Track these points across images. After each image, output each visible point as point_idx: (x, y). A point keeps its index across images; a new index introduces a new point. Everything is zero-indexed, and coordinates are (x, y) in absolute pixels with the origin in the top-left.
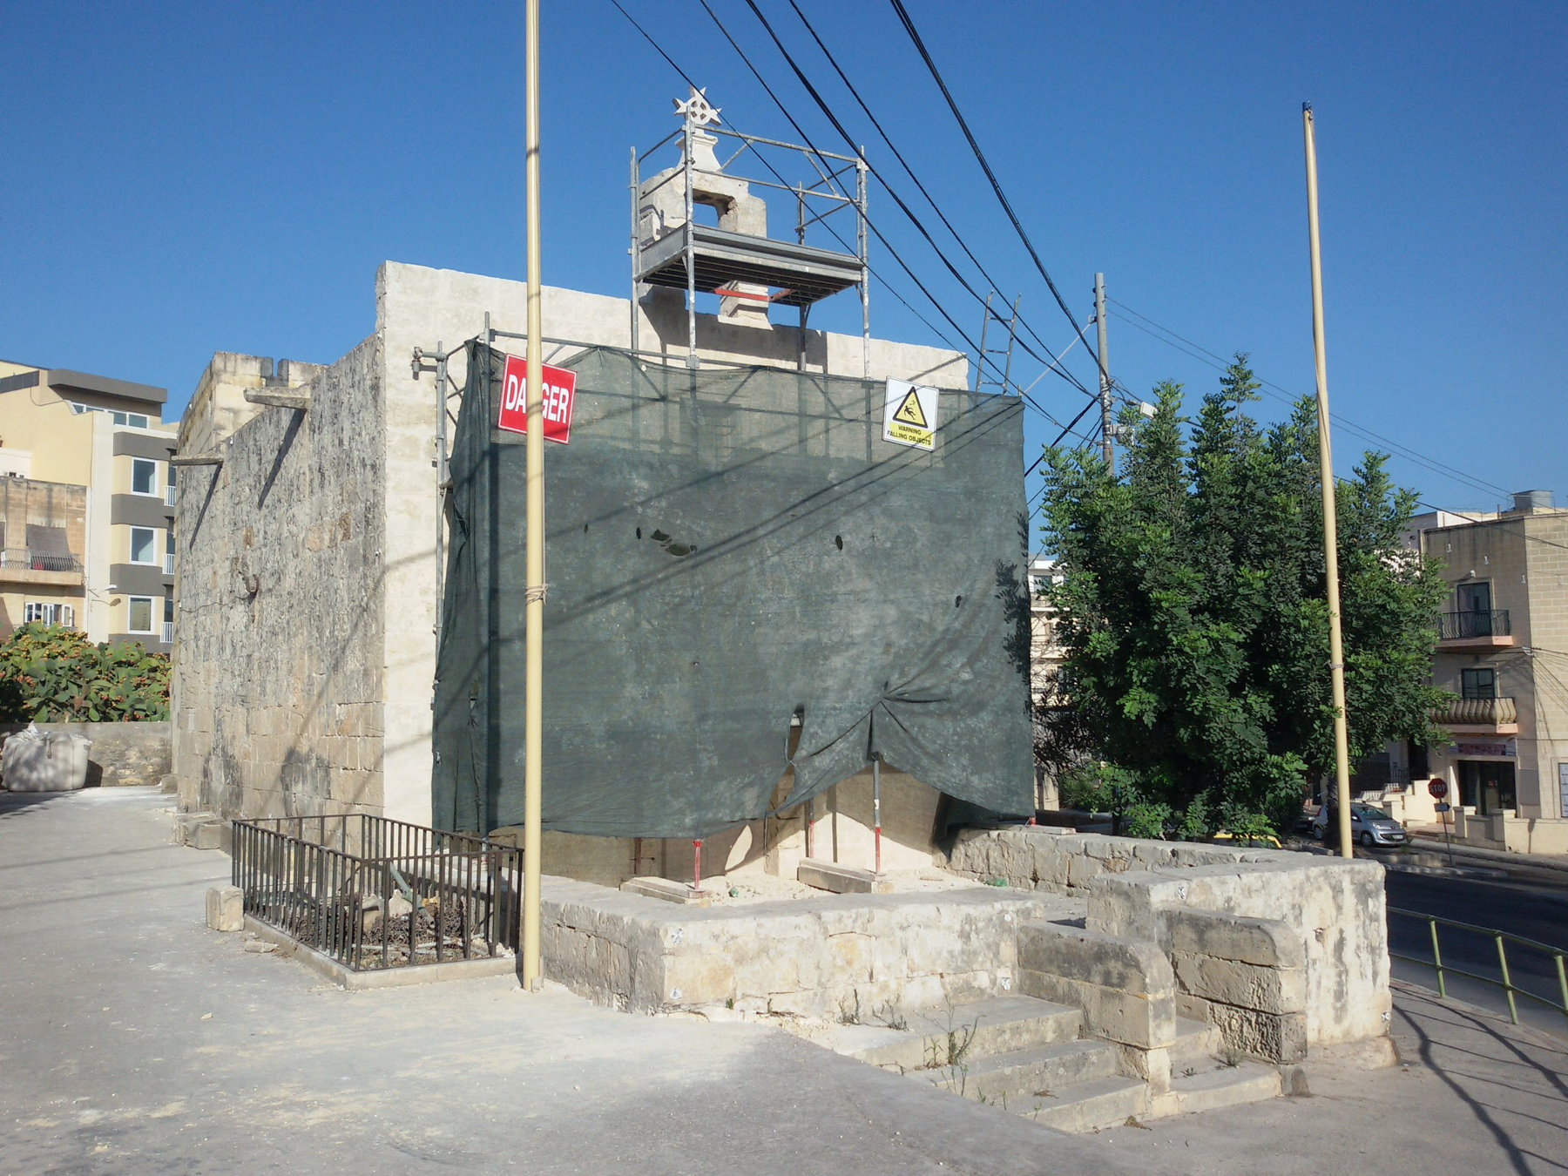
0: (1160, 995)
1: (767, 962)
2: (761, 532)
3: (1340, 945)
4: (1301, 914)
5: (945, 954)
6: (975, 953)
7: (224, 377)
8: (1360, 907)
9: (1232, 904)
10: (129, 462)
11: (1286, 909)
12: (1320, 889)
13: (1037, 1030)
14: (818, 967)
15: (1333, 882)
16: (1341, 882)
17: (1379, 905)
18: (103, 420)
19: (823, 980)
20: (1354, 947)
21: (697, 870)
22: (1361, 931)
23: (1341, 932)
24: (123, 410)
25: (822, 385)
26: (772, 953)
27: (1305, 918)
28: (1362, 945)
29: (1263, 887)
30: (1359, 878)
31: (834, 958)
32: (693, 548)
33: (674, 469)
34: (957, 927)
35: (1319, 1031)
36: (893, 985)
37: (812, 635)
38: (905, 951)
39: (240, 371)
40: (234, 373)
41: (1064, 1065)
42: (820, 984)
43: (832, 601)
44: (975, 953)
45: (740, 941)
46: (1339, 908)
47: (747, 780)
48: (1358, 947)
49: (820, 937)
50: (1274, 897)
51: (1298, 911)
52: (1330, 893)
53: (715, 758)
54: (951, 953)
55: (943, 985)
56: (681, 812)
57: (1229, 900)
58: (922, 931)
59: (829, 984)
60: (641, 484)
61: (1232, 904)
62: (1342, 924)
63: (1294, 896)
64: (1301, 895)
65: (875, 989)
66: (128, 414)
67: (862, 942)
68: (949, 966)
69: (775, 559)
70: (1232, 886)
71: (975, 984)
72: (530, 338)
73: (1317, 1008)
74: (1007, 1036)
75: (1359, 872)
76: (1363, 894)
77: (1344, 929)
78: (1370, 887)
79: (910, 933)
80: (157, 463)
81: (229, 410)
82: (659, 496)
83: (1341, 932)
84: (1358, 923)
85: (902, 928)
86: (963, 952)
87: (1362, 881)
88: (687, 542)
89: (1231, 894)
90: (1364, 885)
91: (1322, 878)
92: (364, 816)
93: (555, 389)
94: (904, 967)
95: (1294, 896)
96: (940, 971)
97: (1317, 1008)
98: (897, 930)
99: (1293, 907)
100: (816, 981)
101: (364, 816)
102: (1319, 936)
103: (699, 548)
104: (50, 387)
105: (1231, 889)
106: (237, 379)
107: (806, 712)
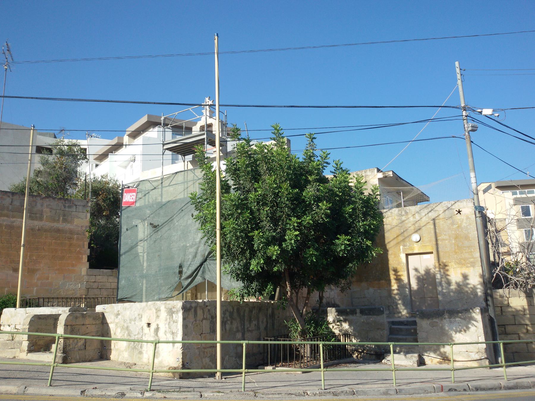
2: (175, 216)
3: (157, 329)
4: (142, 317)
8: (168, 317)
9: (119, 312)
10: (518, 208)
11: (136, 315)
12: (150, 309)
15: (156, 307)
16: (160, 307)
17: (179, 317)
18: (508, 195)
20: (164, 331)
21: (488, 342)
22: (167, 326)
23: (158, 325)
24: (515, 190)
25: (193, 171)
27: (143, 319)
28: (167, 331)
29: (130, 308)
30: (170, 306)
32: (158, 225)
33: (155, 206)
37: (184, 243)
41: (19, 343)
43: (190, 233)
46: (158, 317)
47: (169, 287)
48: (166, 331)
50: (133, 311)
51: (140, 316)
52: (155, 311)
53: (162, 281)
56: (154, 295)
57: (118, 311)
60: (148, 212)
61: (119, 312)
62: (158, 322)
66: (526, 190)
69: (177, 224)
70: (120, 307)
72: (470, 142)
73: (147, 351)
75: (169, 304)
76: (171, 312)
78: (174, 310)
80: (530, 206)
82: (152, 214)
83: (158, 325)
84: (166, 323)
87: (170, 307)
88: (157, 224)
89: (119, 309)
90: (171, 309)
91: (152, 306)
93: (133, 194)
97: (147, 351)
99: (139, 315)
102: (149, 325)
103: (160, 225)
104: (496, 188)
105: (119, 308)
107: (183, 266)
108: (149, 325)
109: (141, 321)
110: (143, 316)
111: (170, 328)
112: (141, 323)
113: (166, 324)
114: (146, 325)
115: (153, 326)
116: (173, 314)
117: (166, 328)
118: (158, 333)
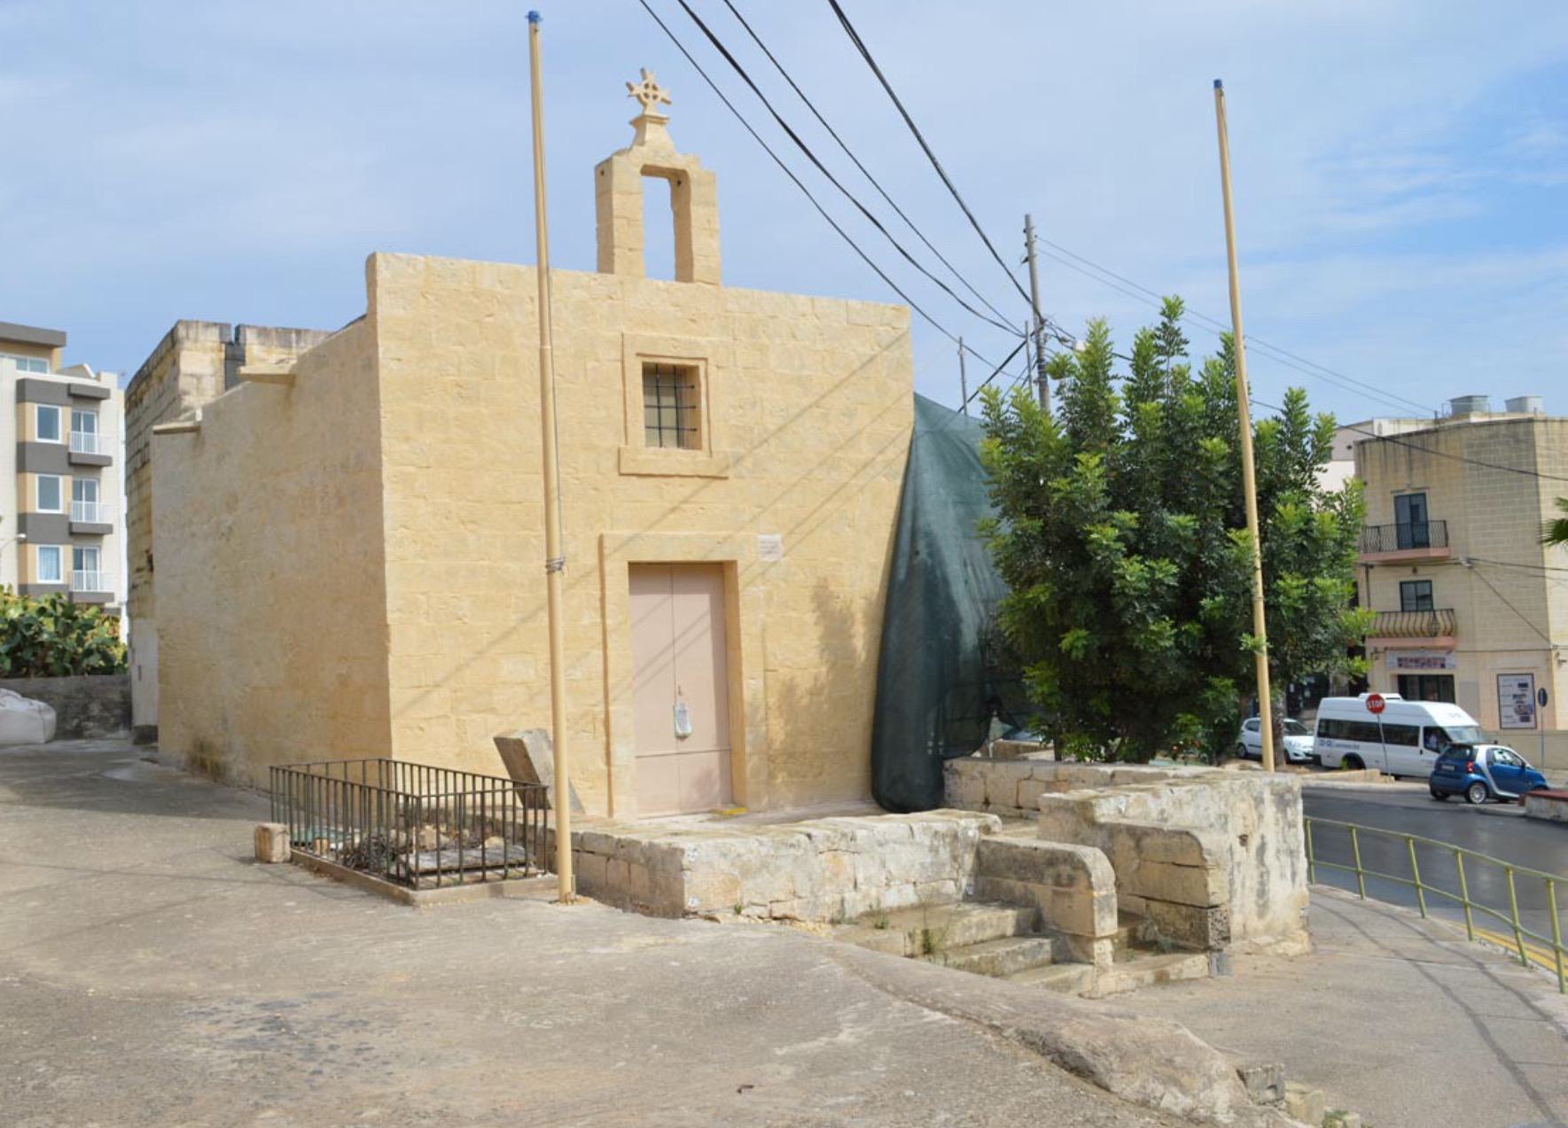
0: (1103, 893)
1: (767, 876)
3: (1262, 849)
4: (1226, 823)
5: (917, 867)
6: (943, 865)
7: (187, 344)
8: (1279, 815)
9: (1165, 815)
13: (998, 926)
14: (810, 879)
15: (1255, 794)
19: (816, 889)
23: (1263, 837)
26: (772, 867)
27: (1230, 826)
31: (824, 871)
34: (927, 843)
35: (1244, 926)
36: (874, 892)
38: (883, 864)
39: (201, 338)
40: (196, 340)
42: (812, 892)
44: (943, 865)
45: (745, 858)
46: (1261, 817)
49: (811, 854)
50: (1202, 808)
51: (1223, 820)
52: (1252, 802)
54: (922, 865)
55: (916, 892)
57: (1162, 812)
58: (897, 846)
59: (820, 893)
61: (1165, 815)
63: (1219, 808)
64: (1226, 805)
65: (859, 897)
67: (846, 858)
68: (921, 876)
71: (944, 890)
73: (1242, 906)
74: (974, 931)
77: (1265, 834)
79: (887, 849)
81: (192, 375)
83: (1263, 837)
85: (881, 845)
86: (932, 864)
89: (1165, 807)
92: (380, 761)
94: (883, 878)
95: (1219, 808)
96: (913, 880)
98: (876, 847)
100: (809, 889)
101: (380, 761)
102: (1244, 840)
106: (199, 345)
108: (1244, 840)
109: (1226, 831)
110: (1229, 819)
111: (1285, 841)
112: (1225, 837)
113: (1278, 833)
114: (1237, 843)
115: (1254, 842)
116: (1288, 810)
117: (1278, 841)
118: (1265, 858)
